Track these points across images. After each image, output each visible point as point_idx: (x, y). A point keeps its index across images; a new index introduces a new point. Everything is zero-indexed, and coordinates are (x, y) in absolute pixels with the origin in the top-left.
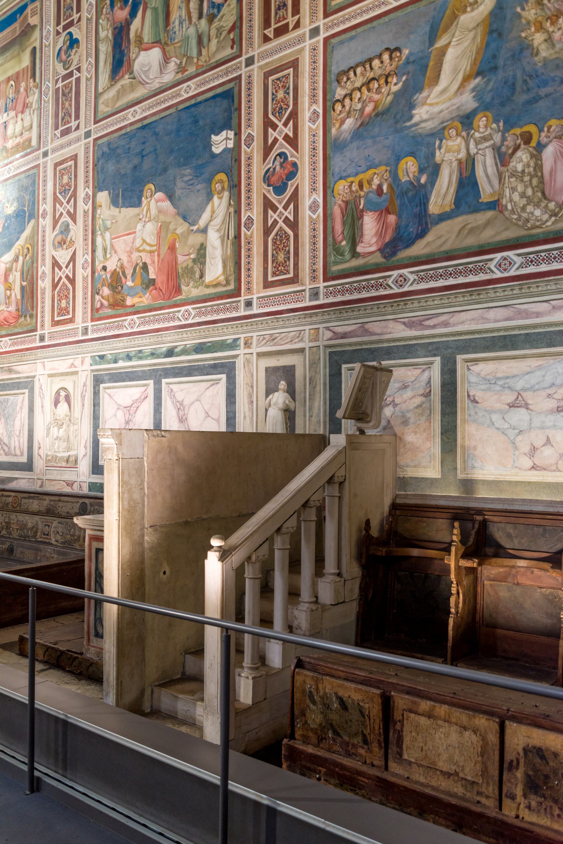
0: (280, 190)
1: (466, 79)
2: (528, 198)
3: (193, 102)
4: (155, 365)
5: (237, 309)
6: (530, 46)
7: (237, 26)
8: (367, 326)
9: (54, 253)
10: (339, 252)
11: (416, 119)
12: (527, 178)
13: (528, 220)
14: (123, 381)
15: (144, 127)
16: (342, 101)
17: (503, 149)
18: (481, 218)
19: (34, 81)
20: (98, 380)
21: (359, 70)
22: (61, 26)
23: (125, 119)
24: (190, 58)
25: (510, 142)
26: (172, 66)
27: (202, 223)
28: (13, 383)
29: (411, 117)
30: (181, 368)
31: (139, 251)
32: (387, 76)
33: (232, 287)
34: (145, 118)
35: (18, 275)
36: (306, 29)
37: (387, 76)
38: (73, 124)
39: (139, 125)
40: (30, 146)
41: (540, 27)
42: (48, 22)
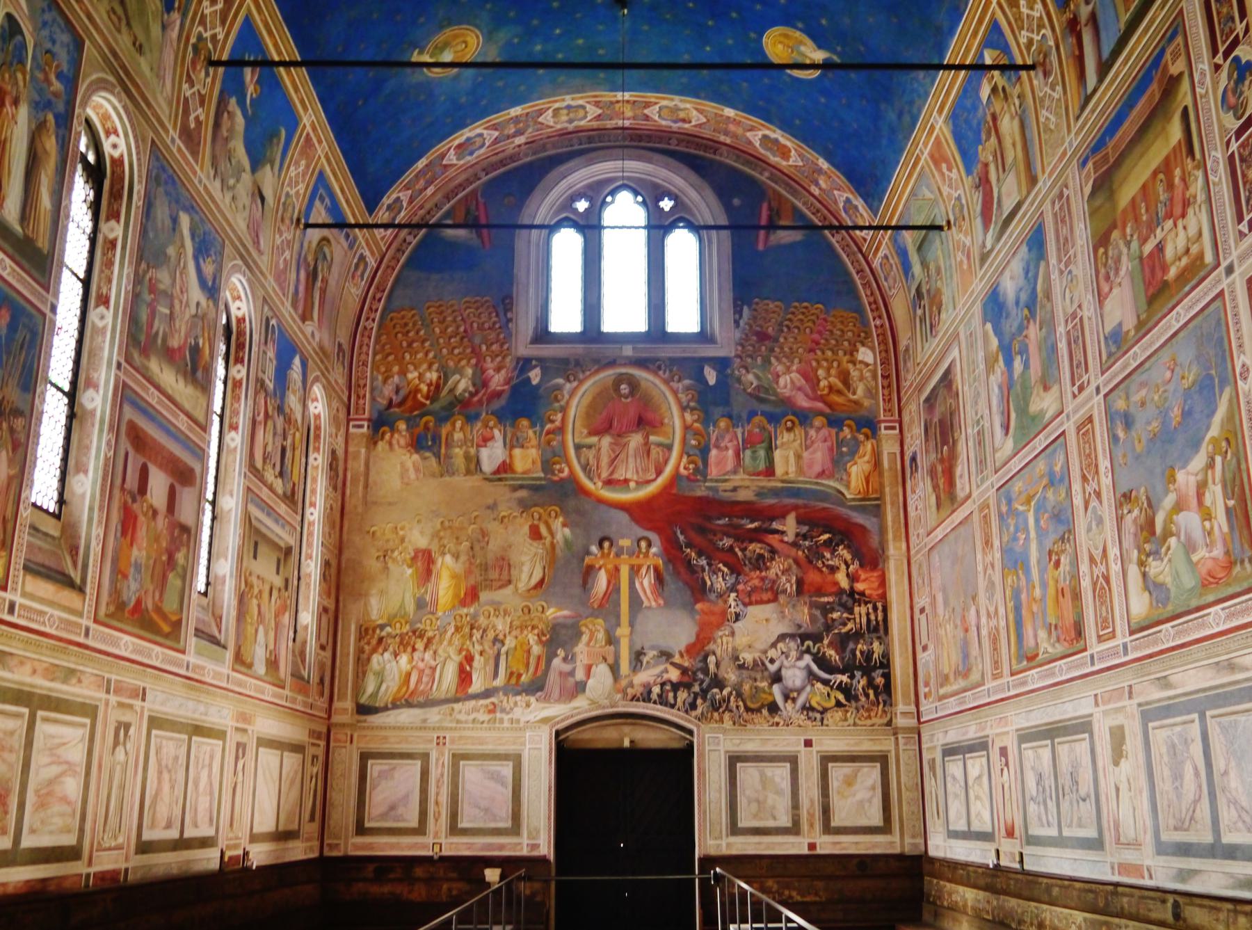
19: (1193, 158)
22: (1220, 55)
28: (1240, 690)
35: (1218, 489)
40: (1203, 265)
42: (1199, 57)
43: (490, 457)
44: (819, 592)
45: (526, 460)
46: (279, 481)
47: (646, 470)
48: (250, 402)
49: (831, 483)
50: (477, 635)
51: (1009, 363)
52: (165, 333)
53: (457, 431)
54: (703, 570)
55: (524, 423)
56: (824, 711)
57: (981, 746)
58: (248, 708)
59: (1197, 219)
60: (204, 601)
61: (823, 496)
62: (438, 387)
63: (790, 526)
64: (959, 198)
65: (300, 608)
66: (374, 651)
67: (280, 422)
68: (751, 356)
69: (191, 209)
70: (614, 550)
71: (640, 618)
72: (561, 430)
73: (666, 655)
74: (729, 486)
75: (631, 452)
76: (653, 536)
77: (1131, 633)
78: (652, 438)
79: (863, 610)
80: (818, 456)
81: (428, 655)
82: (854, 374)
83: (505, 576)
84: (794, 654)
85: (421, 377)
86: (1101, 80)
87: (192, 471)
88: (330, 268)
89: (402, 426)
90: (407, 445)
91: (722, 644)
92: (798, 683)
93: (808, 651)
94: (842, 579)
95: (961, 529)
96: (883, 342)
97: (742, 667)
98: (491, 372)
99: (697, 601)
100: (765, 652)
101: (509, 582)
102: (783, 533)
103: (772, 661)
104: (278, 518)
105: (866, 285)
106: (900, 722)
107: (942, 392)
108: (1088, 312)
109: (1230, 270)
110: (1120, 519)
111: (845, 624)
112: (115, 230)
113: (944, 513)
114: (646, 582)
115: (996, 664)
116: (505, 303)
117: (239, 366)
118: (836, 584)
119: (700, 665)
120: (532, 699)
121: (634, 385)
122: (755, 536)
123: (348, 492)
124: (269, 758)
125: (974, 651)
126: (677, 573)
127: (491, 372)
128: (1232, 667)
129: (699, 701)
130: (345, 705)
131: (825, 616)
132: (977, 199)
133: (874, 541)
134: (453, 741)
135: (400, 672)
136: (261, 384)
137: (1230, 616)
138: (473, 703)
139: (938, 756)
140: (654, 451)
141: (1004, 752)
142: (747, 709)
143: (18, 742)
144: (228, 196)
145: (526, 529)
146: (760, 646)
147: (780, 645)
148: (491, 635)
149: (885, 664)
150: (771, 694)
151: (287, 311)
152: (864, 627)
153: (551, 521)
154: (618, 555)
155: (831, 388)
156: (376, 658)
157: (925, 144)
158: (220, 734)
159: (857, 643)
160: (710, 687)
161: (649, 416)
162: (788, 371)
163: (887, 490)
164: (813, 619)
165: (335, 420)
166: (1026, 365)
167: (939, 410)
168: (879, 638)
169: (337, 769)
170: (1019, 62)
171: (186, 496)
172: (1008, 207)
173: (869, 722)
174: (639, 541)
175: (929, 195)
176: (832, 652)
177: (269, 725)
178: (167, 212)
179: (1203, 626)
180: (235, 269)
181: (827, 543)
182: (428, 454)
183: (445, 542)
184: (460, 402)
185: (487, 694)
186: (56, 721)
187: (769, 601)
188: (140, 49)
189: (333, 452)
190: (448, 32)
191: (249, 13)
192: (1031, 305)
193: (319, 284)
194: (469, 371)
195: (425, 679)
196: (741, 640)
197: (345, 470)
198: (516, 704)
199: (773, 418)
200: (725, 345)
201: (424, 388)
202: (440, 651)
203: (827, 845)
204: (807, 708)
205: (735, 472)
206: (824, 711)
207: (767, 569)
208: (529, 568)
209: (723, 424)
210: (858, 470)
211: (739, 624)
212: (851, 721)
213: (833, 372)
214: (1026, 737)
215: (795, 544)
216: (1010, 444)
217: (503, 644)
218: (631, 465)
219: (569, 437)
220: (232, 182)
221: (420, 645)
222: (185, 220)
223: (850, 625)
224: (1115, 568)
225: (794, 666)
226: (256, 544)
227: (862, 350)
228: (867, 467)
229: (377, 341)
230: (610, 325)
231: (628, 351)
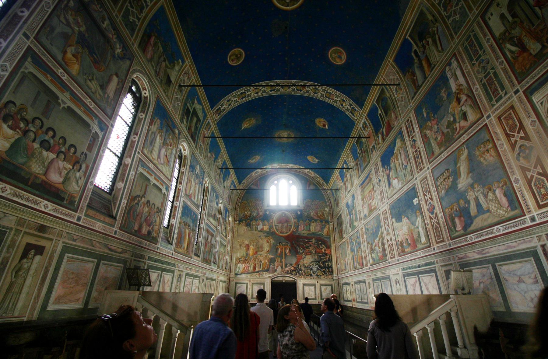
0: (432, 213)
1: (468, 174)
2: (497, 207)
4: (427, 269)
5: (431, 251)
6: (481, 162)
7: (411, 170)
8: (467, 254)
10: (452, 231)
11: (459, 188)
12: (494, 201)
13: (499, 215)
16: (440, 186)
17: (484, 193)
18: (486, 216)
20: (404, 276)
21: (441, 177)
23: (394, 198)
24: (403, 180)
25: (486, 191)
26: (400, 183)
27: (417, 225)
29: (458, 187)
30: (423, 271)
32: (448, 177)
33: (428, 244)
36: (426, 168)
37: (448, 177)
38: (384, 201)
41: (481, 156)
44: (319, 253)
45: (266, 228)
50: (257, 260)
51: (350, 215)
57: (348, 284)
58: (219, 275)
59: (375, 201)
61: (319, 235)
63: (313, 241)
72: (272, 223)
73: (291, 265)
76: (289, 242)
80: (318, 228)
89: (244, 222)
91: (301, 263)
96: (329, 207)
97: (305, 267)
99: (297, 254)
105: (326, 197)
106: (335, 278)
108: (361, 210)
109: (380, 210)
110: (368, 246)
114: (287, 251)
115: (350, 269)
122: (307, 242)
124: (221, 284)
125: (347, 266)
128: (384, 273)
130: (233, 273)
132: (344, 186)
133: (329, 243)
137: (383, 265)
139: (342, 285)
140: (289, 226)
141: (352, 285)
143: (191, 283)
146: (308, 263)
148: (259, 260)
149: (332, 267)
151: (227, 204)
156: (238, 265)
158: (214, 280)
165: (233, 221)
166: (353, 216)
171: (213, 239)
172: (349, 189)
181: (320, 244)
192: (353, 207)
196: (305, 262)
199: (310, 221)
204: (317, 275)
206: (320, 276)
208: (266, 248)
209: (301, 221)
210: (325, 230)
214: (356, 282)
215: (314, 244)
216: (351, 230)
221: (247, 262)
222: (215, 194)
224: (367, 254)
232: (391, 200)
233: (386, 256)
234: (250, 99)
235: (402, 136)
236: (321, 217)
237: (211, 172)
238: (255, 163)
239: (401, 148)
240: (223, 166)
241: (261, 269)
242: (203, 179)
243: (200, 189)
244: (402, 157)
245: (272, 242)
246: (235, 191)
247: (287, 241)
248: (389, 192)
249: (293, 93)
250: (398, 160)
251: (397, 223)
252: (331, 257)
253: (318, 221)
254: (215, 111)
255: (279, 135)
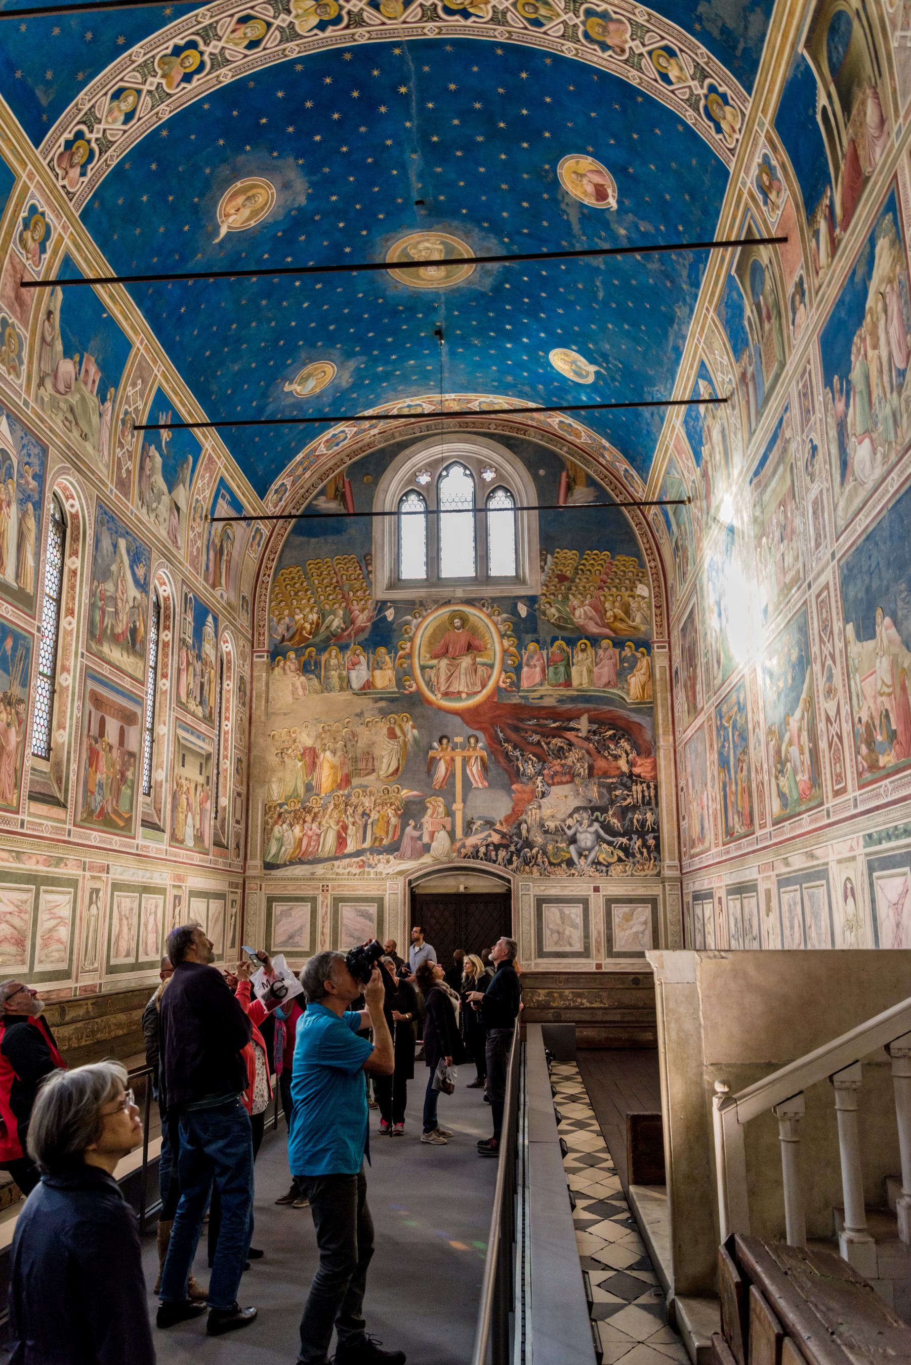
3: (898, 497)
9: (826, 705)
14: (887, 868)
15: (867, 539)
31: (882, 695)
34: (868, 526)
39: (864, 537)
43: (357, 677)
44: (606, 775)
45: (384, 679)
46: (200, 708)
47: (474, 684)
48: (176, 657)
49: (615, 691)
50: (350, 810)
52: (112, 625)
53: (332, 657)
54: (518, 759)
55: (382, 650)
56: (609, 865)
57: (709, 895)
60: (148, 800)
62: (318, 625)
63: (583, 724)
64: (694, 482)
65: (220, 794)
66: (276, 823)
67: (198, 666)
68: (553, 594)
69: (127, 534)
70: (451, 745)
71: (470, 796)
72: (409, 656)
73: (489, 824)
74: (537, 695)
75: (463, 671)
76: (480, 734)
77: (774, 825)
78: (478, 660)
79: (639, 788)
80: (605, 671)
81: (314, 826)
82: (634, 605)
83: (370, 766)
84: (586, 822)
85: (305, 618)
86: (757, 425)
87: (135, 714)
88: (232, 544)
89: (292, 655)
90: (297, 670)
91: (532, 816)
92: (589, 844)
93: (597, 820)
94: (623, 764)
95: (699, 733)
97: (546, 832)
98: (357, 612)
100: (564, 821)
101: (374, 770)
102: (578, 730)
103: (569, 828)
104: (199, 735)
106: (667, 873)
107: (689, 626)
109: (809, 586)
110: (767, 744)
111: (625, 799)
112: (73, 563)
113: (692, 719)
114: (474, 770)
116: (366, 560)
117: (167, 632)
118: (619, 768)
119: (515, 831)
120: (391, 857)
121: (464, 620)
122: (557, 733)
123: (254, 706)
126: (497, 762)
127: (357, 612)
128: (812, 856)
129: (515, 858)
130: (255, 863)
131: (610, 794)
133: (648, 735)
134: (333, 889)
135: (295, 838)
136: (183, 641)
137: (811, 822)
138: (348, 860)
139: (690, 899)
140: (480, 669)
141: (720, 898)
142: (551, 864)
144: (153, 516)
145: (385, 731)
146: (560, 816)
147: (576, 816)
149: (656, 829)
150: (569, 852)
151: (200, 584)
152: (640, 801)
153: (403, 724)
154: (453, 749)
155: (615, 617)
156: (277, 828)
157: (671, 438)
159: (634, 813)
160: (522, 848)
161: (476, 643)
162: (582, 604)
163: (659, 695)
164: (601, 795)
165: (242, 655)
167: (688, 639)
168: (651, 809)
169: (250, 909)
170: (720, 397)
171: (132, 733)
173: (643, 873)
174: (469, 738)
175: (677, 475)
176: (615, 821)
177: (198, 881)
178: (109, 541)
179: (801, 826)
180: (160, 565)
181: (612, 738)
182: (311, 676)
183: (326, 741)
184: (334, 636)
185: (358, 853)
186: (52, 892)
187: (567, 782)
188: (85, 437)
189: (242, 678)
190: (310, 367)
191: (160, 383)
193: (225, 557)
194: (341, 612)
195: (313, 843)
196: (546, 812)
197: (252, 690)
198: (379, 861)
199: (571, 642)
200: (534, 584)
201: (308, 626)
202: (324, 823)
203: (610, 965)
204: (596, 863)
205: (541, 684)
206: (609, 865)
207: (566, 758)
209: (532, 646)
210: (635, 681)
211: (544, 800)
212: (629, 873)
213: (617, 604)
215: (587, 739)
217: (369, 816)
218: (463, 682)
219: (416, 661)
220: (154, 505)
221: (309, 818)
222: (122, 543)
223: (629, 800)
224: (766, 778)
225: (586, 831)
226: (184, 756)
227: (640, 586)
228: (643, 678)
229: (271, 593)
230: (448, 570)
231: (459, 593)
232: (847, 540)
233: (820, 786)
234: (226, 76)
235: (895, 221)
236: (619, 625)
237: (88, 446)
238: (319, 396)
239: (890, 281)
240: (153, 415)
241: (367, 845)
242: (40, 478)
243: (31, 523)
244: (892, 331)
245: (410, 736)
246: (239, 529)
247: (471, 732)
248: (842, 504)
249: (430, 31)
250: (875, 346)
251: (859, 644)
252: (656, 788)
253: (605, 643)
254: (59, 148)
255: (404, 252)
